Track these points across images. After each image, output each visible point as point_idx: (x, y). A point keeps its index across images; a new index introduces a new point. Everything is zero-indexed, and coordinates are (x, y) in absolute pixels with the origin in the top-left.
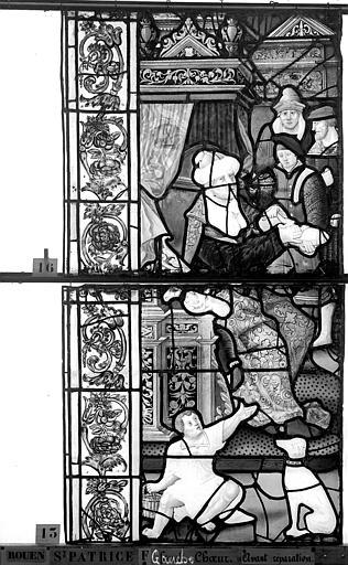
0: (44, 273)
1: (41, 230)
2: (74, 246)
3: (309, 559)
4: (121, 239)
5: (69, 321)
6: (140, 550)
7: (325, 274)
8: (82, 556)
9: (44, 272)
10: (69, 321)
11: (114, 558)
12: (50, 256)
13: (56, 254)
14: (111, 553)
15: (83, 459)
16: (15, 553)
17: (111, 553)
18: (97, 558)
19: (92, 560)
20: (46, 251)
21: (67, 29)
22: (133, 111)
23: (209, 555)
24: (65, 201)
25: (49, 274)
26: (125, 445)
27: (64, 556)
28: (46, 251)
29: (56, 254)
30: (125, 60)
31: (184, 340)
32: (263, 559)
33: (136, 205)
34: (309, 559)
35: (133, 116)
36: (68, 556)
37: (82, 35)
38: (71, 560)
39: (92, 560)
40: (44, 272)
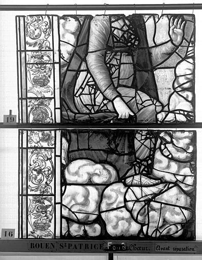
0: (10, 123)
1: (10, 105)
3: (193, 249)
7: (190, 122)
8: (75, 245)
9: (9, 123)
11: (93, 247)
12: (13, 114)
13: (15, 113)
14: (92, 245)
17: (92, 245)
18: (83, 247)
19: (81, 248)
20: (11, 111)
23: (137, 246)
25: (13, 123)
27: (66, 246)
28: (11, 111)
29: (15, 113)
32: (167, 249)
34: (193, 249)
36: (67, 245)
38: (69, 248)
39: (81, 248)
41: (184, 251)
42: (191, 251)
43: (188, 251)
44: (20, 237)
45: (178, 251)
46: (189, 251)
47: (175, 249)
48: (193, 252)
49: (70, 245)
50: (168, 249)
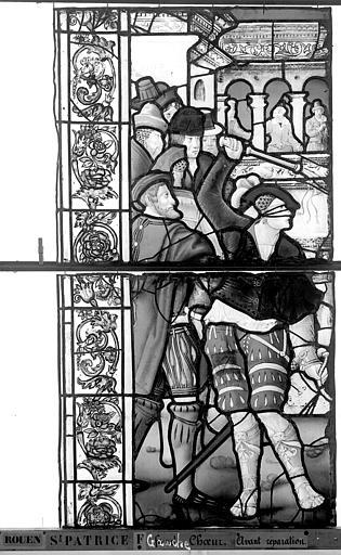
1: (33, 224)
2: (68, 327)
4: (112, 247)
5: (65, 497)
6: (135, 534)
10: (65, 497)
11: (110, 539)
15: (79, 461)
16: (14, 539)
18: (92, 541)
20: (40, 240)
21: (61, 179)
22: (127, 308)
23: (203, 538)
24: (58, 210)
26: (119, 447)
30: (120, 340)
31: (180, 367)
32: (257, 542)
33: (129, 311)
35: (127, 313)
36: (64, 540)
37: (74, 48)
40: (40, 266)
41: (285, 546)
42: (298, 545)
43: (292, 546)
44: (63, 524)
45: (276, 546)
46: (295, 546)
47: (269, 542)
48: (302, 546)
49: (68, 539)
50: (257, 542)
